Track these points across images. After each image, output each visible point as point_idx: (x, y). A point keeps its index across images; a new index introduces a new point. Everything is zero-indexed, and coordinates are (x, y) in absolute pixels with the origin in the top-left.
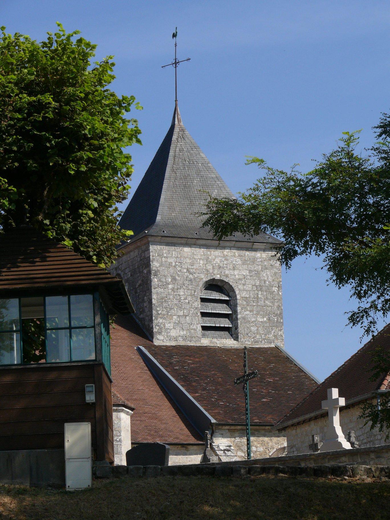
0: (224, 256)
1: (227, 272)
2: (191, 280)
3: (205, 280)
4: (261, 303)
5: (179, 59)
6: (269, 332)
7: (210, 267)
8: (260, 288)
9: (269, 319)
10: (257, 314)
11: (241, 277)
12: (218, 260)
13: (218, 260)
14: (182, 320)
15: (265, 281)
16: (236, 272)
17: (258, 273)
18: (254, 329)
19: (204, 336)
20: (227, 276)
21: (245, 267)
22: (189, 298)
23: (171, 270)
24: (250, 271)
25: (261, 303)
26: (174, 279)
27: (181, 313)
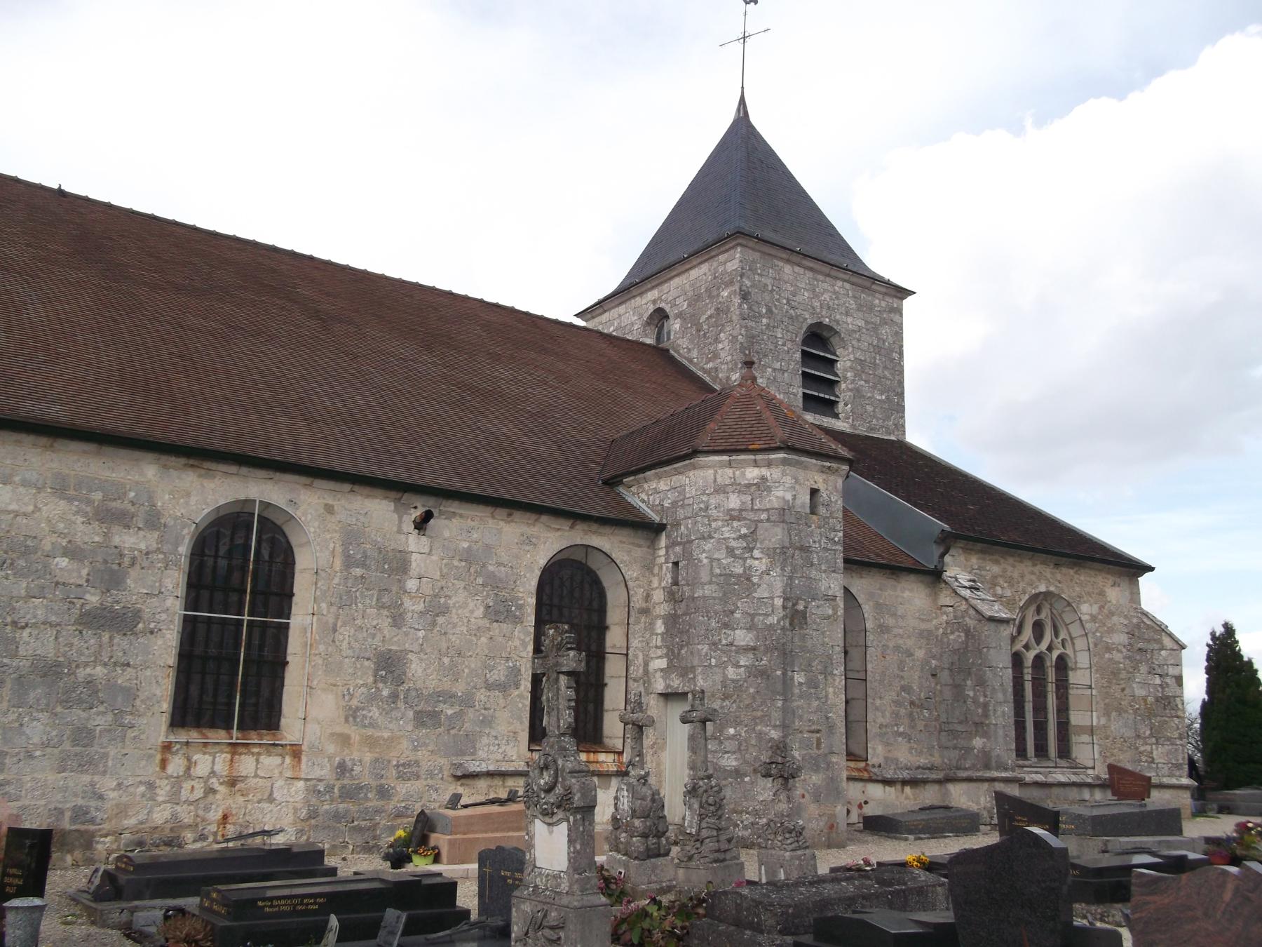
0: (835, 292)
1: (838, 317)
2: (791, 318)
3: (810, 321)
4: (879, 372)
5: (749, 31)
6: (888, 418)
7: (817, 304)
8: (878, 349)
9: (887, 398)
10: (874, 387)
11: (856, 329)
12: (826, 296)
13: (826, 296)
14: (779, 375)
15: (884, 341)
16: (849, 320)
17: (875, 328)
18: (869, 408)
19: (805, 409)
20: (838, 322)
21: (860, 314)
22: (789, 345)
23: (767, 296)
24: (867, 322)
25: (879, 372)
26: (769, 310)
27: (777, 365)
